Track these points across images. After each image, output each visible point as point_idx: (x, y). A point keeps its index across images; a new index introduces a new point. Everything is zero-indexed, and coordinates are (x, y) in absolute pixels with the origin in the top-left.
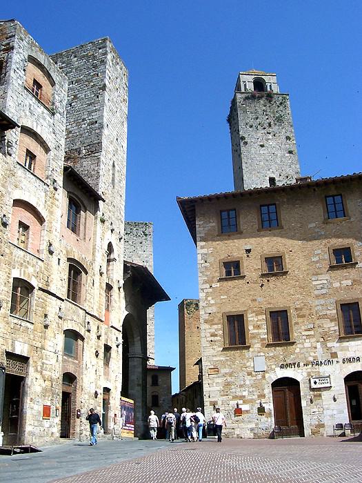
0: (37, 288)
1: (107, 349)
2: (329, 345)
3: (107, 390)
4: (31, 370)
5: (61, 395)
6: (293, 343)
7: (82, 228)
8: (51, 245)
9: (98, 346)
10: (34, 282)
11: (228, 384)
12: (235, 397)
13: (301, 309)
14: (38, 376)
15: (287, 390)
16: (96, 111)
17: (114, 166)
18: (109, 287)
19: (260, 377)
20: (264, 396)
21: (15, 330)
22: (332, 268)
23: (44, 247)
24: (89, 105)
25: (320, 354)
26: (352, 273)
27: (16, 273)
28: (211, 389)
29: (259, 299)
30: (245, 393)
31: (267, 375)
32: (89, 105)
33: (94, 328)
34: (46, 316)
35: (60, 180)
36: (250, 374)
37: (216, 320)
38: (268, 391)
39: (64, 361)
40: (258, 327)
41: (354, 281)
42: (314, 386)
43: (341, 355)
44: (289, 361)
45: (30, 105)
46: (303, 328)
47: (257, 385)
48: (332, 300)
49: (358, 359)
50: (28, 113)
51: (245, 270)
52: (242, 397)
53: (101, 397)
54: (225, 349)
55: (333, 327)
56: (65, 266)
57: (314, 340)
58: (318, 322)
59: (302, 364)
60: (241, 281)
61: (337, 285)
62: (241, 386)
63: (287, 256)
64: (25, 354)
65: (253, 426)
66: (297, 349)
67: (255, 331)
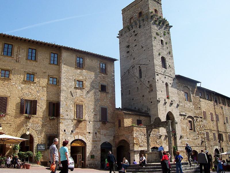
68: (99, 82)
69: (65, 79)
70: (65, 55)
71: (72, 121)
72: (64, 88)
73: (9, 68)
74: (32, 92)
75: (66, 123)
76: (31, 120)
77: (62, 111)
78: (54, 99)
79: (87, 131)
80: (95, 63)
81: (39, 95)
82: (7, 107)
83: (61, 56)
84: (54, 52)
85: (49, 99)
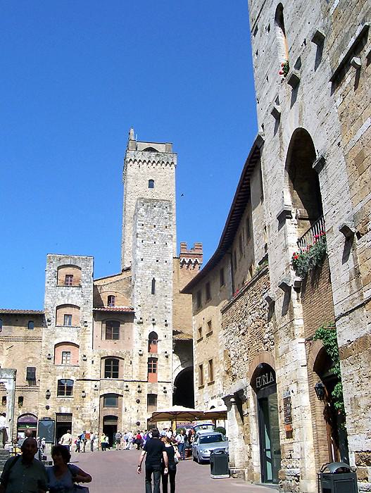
0: (75, 380)
10: (73, 378)
14: (79, 421)
17: (154, 281)
21: (61, 403)
23: (80, 358)
27: (60, 378)
35: (90, 319)
46: (217, 371)
50: (60, 298)
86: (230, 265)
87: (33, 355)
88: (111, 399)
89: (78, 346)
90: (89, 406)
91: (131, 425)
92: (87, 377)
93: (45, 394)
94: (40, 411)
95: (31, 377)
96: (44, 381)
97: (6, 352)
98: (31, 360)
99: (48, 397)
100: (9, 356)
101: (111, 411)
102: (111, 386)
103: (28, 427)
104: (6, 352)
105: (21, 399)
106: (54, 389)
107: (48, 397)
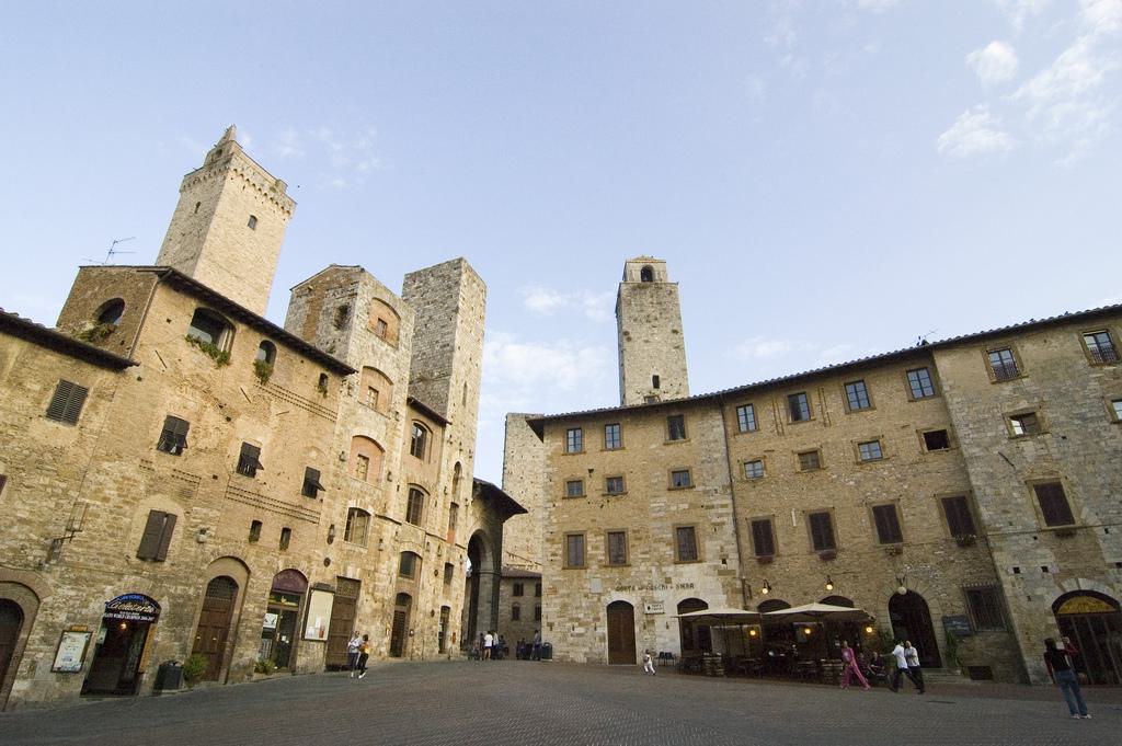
0: (373, 515)
1: (449, 566)
2: (664, 569)
3: (445, 609)
4: (362, 592)
5: (393, 615)
6: (629, 566)
7: (427, 451)
8: (390, 473)
9: (438, 565)
10: (370, 510)
11: (565, 606)
12: (571, 620)
13: (638, 531)
14: (369, 598)
15: (621, 615)
16: (448, 333)
17: (465, 385)
18: (454, 506)
19: (595, 599)
20: (599, 619)
21: (349, 555)
22: (669, 490)
23: (384, 475)
24: (443, 327)
25: (655, 577)
26: (689, 496)
27: (352, 504)
28: (550, 609)
29: (598, 519)
30: (581, 616)
31: (602, 598)
32: (443, 327)
33: (434, 548)
34: (381, 540)
36: (586, 596)
37: (557, 539)
38: (603, 614)
39: (397, 582)
40: (596, 548)
41: (691, 504)
42: (647, 611)
43: (675, 581)
44: (624, 584)
45: (373, 345)
47: (593, 608)
48: (669, 523)
49: (692, 586)
50: (370, 353)
51: (587, 491)
52: (578, 620)
53: (438, 615)
54: (564, 569)
55: (668, 552)
56: (405, 491)
57: (648, 564)
58: (655, 545)
59: (636, 588)
60: (584, 501)
61: (673, 508)
62: (577, 608)
63: (627, 477)
64: (357, 578)
65: (587, 650)
66: (633, 571)
67: (594, 552)
68: (1099, 394)
69: (967, 425)
70: (944, 363)
71: (1035, 538)
72: (976, 451)
73: (815, 445)
74: (887, 484)
75: (1015, 548)
76: (905, 557)
77: (985, 513)
78: (952, 488)
79: (1108, 561)
80: (1062, 346)
81: (906, 487)
82: (835, 536)
83: (935, 371)
84: (914, 367)
85: (940, 491)
86: (720, 422)
87: (320, 445)
88: (409, 563)
89: (382, 450)
90: (385, 571)
91: (425, 613)
92: (390, 514)
93: (325, 532)
94: (315, 568)
95: (311, 487)
96: (329, 506)
97: (274, 421)
98: (313, 454)
99: (330, 540)
100: (280, 430)
101: (406, 589)
102: (412, 539)
103: (283, 600)
104: (274, 421)
105: (286, 531)
106: (340, 523)
107: (330, 540)
